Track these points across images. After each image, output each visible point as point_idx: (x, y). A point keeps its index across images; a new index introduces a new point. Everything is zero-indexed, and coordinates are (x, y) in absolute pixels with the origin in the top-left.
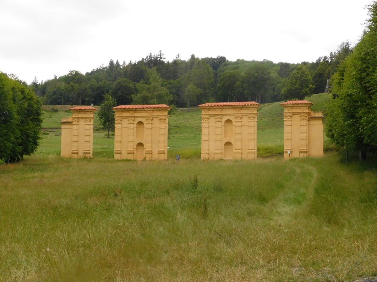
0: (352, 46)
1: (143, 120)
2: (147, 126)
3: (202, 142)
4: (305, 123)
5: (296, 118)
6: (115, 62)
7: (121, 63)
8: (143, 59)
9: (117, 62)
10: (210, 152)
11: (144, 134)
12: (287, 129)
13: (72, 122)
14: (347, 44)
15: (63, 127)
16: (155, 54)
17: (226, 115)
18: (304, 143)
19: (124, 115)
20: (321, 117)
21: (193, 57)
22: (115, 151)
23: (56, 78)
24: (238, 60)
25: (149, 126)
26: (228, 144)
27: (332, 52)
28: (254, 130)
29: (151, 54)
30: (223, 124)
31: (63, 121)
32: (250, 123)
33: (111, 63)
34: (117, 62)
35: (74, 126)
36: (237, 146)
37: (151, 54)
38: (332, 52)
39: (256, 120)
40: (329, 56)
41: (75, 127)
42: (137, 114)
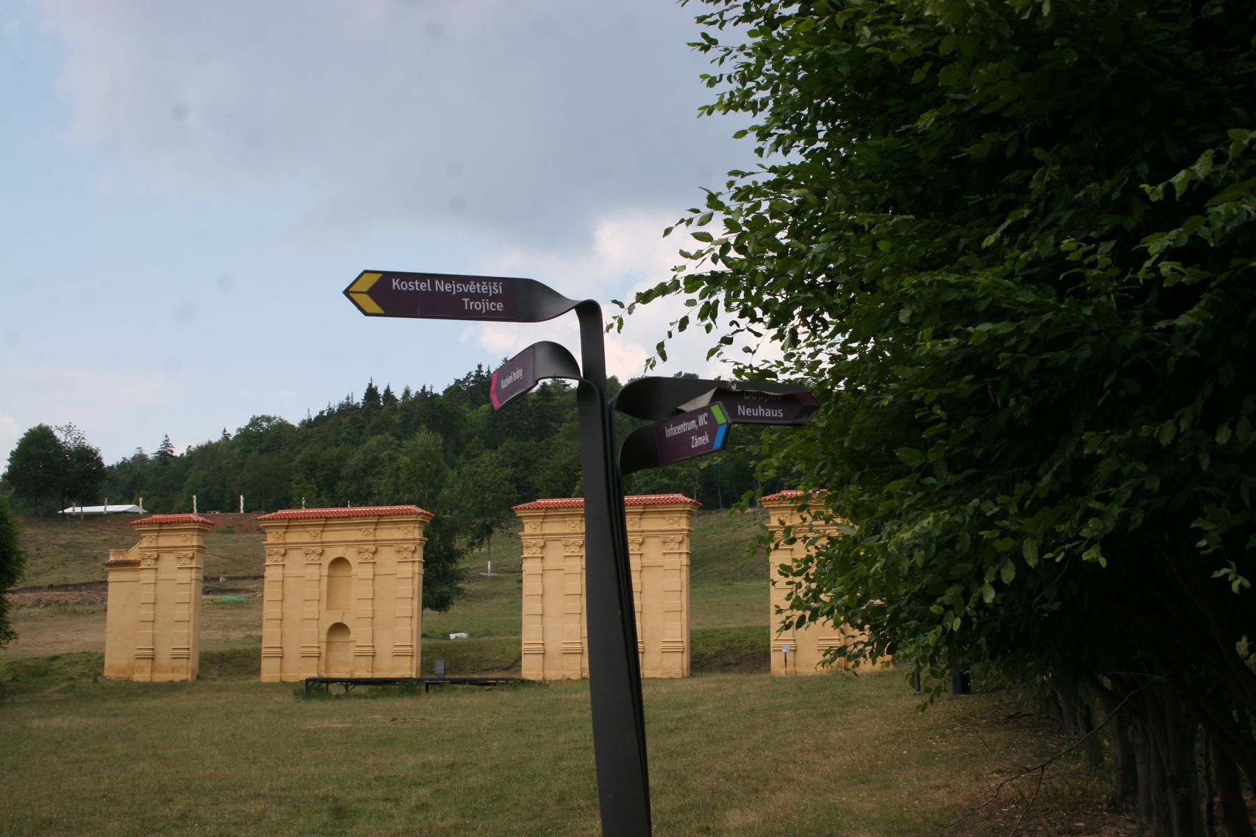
1: (351, 555)
2: (361, 571)
6: (381, 392)
7: (398, 395)
8: (458, 381)
9: (387, 391)
10: (549, 649)
15: (112, 577)
22: (264, 650)
23: (226, 437)
25: (367, 571)
29: (480, 366)
31: (112, 558)
32: (669, 559)
33: (371, 393)
34: (387, 391)
37: (480, 366)
39: (684, 549)
41: (147, 576)
42: (330, 536)
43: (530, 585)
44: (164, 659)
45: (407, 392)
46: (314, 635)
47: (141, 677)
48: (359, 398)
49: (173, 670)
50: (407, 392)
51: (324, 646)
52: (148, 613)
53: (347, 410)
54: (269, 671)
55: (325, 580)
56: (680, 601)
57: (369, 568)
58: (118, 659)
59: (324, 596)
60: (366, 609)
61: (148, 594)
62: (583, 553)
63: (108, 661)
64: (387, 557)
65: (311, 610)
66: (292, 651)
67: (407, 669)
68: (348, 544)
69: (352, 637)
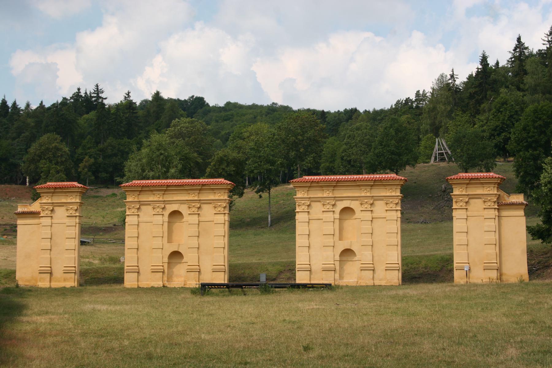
0: (461, 79)
1: (183, 209)
2: (189, 219)
3: (298, 249)
4: (493, 213)
5: (476, 204)
6: (10, 104)
8: (65, 99)
9: (15, 104)
10: (314, 268)
11: (179, 235)
12: (458, 225)
13: (39, 213)
14: (452, 76)
15: (19, 222)
16: (88, 88)
17: (342, 199)
18: (492, 251)
19: (144, 198)
20: (522, 204)
21: (157, 96)
22: (126, 268)
24: (228, 104)
25: (195, 219)
26: (347, 253)
27: (418, 91)
29: (79, 89)
30: (337, 216)
31: (20, 210)
32: (389, 213)
34: (15, 104)
35: (42, 220)
36: (364, 256)
37: (79, 89)
38: (418, 91)
40: (413, 97)
41: (46, 221)
43: (301, 228)
44: (58, 271)
45: (28, 105)
46: (160, 258)
47: (44, 283)
49: (65, 280)
50: (28, 105)
51: (166, 266)
52: (47, 244)
54: (130, 281)
55: (166, 225)
56: (397, 239)
57: (136, 218)
58: (25, 275)
59: (166, 234)
60: (194, 242)
61: (46, 232)
62: (399, 208)
63: (18, 275)
64: (207, 210)
65: (158, 243)
66: (145, 269)
67: (222, 278)
68: (182, 202)
69: (185, 259)
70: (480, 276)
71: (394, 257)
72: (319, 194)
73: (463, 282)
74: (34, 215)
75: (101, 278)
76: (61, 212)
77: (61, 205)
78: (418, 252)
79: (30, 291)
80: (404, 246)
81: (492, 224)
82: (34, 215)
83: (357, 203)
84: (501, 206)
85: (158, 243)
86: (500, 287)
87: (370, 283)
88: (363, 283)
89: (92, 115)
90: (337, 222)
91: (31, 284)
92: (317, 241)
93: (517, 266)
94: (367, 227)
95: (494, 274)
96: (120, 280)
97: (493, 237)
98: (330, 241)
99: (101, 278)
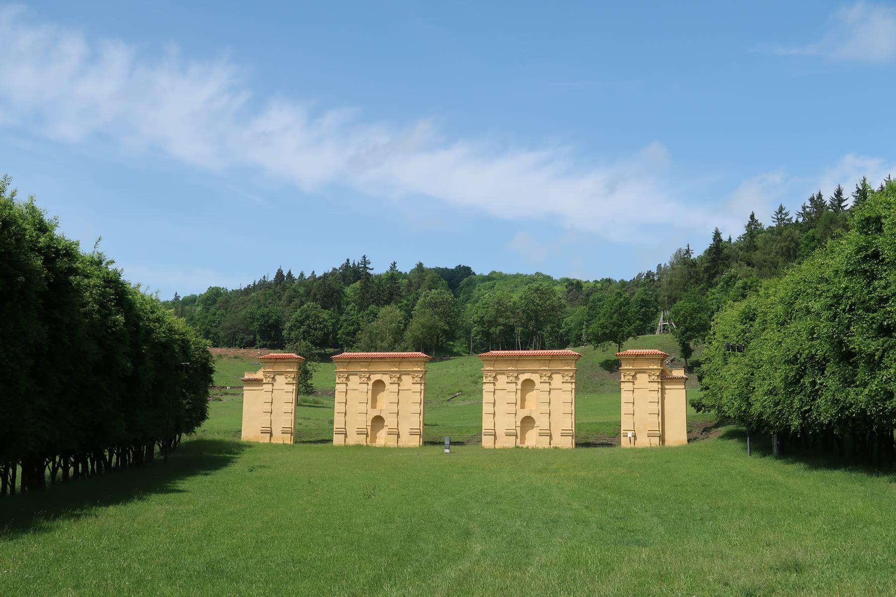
1: (386, 379)
4: (657, 386)
5: (642, 378)
6: (285, 273)
7: (296, 276)
8: (334, 269)
9: (290, 273)
12: (625, 396)
14: (688, 251)
16: (356, 259)
17: (523, 372)
18: (656, 420)
19: (352, 368)
20: (682, 378)
23: (177, 298)
27: (660, 265)
28: (570, 397)
29: (348, 260)
31: (246, 377)
33: (280, 273)
34: (290, 273)
35: (265, 386)
37: (348, 260)
38: (660, 265)
40: (654, 271)
41: (268, 387)
44: (277, 432)
45: (302, 275)
46: (364, 422)
48: (271, 278)
50: (302, 275)
52: (268, 407)
53: (263, 285)
54: (338, 440)
55: (370, 392)
56: (571, 408)
58: (250, 432)
60: (394, 408)
61: (268, 397)
64: (407, 380)
65: (363, 408)
68: (384, 373)
70: (643, 441)
71: (568, 423)
72: (504, 367)
73: (629, 446)
74: (258, 382)
75: (312, 436)
76: (280, 379)
77: (281, 373)
78: (585, 420)
79: (250, 446)
80: (577, 413)
81: (656, 396)
82: (258, 382)
83: (538, 375)
84: (664, 378)
85: (363, 408)
86: (662, 454)
87: (547, 446)
88: (540, 446)
89: (358, 284)
90: (519, 392)
91: (256, 440)
92: (501, 408)
93: (677, 435)
94: (545, 397)
95: (656, 441)
96: (331, 441)
97: (656, 408)
98: (512, 409)
99: (312, 436)
